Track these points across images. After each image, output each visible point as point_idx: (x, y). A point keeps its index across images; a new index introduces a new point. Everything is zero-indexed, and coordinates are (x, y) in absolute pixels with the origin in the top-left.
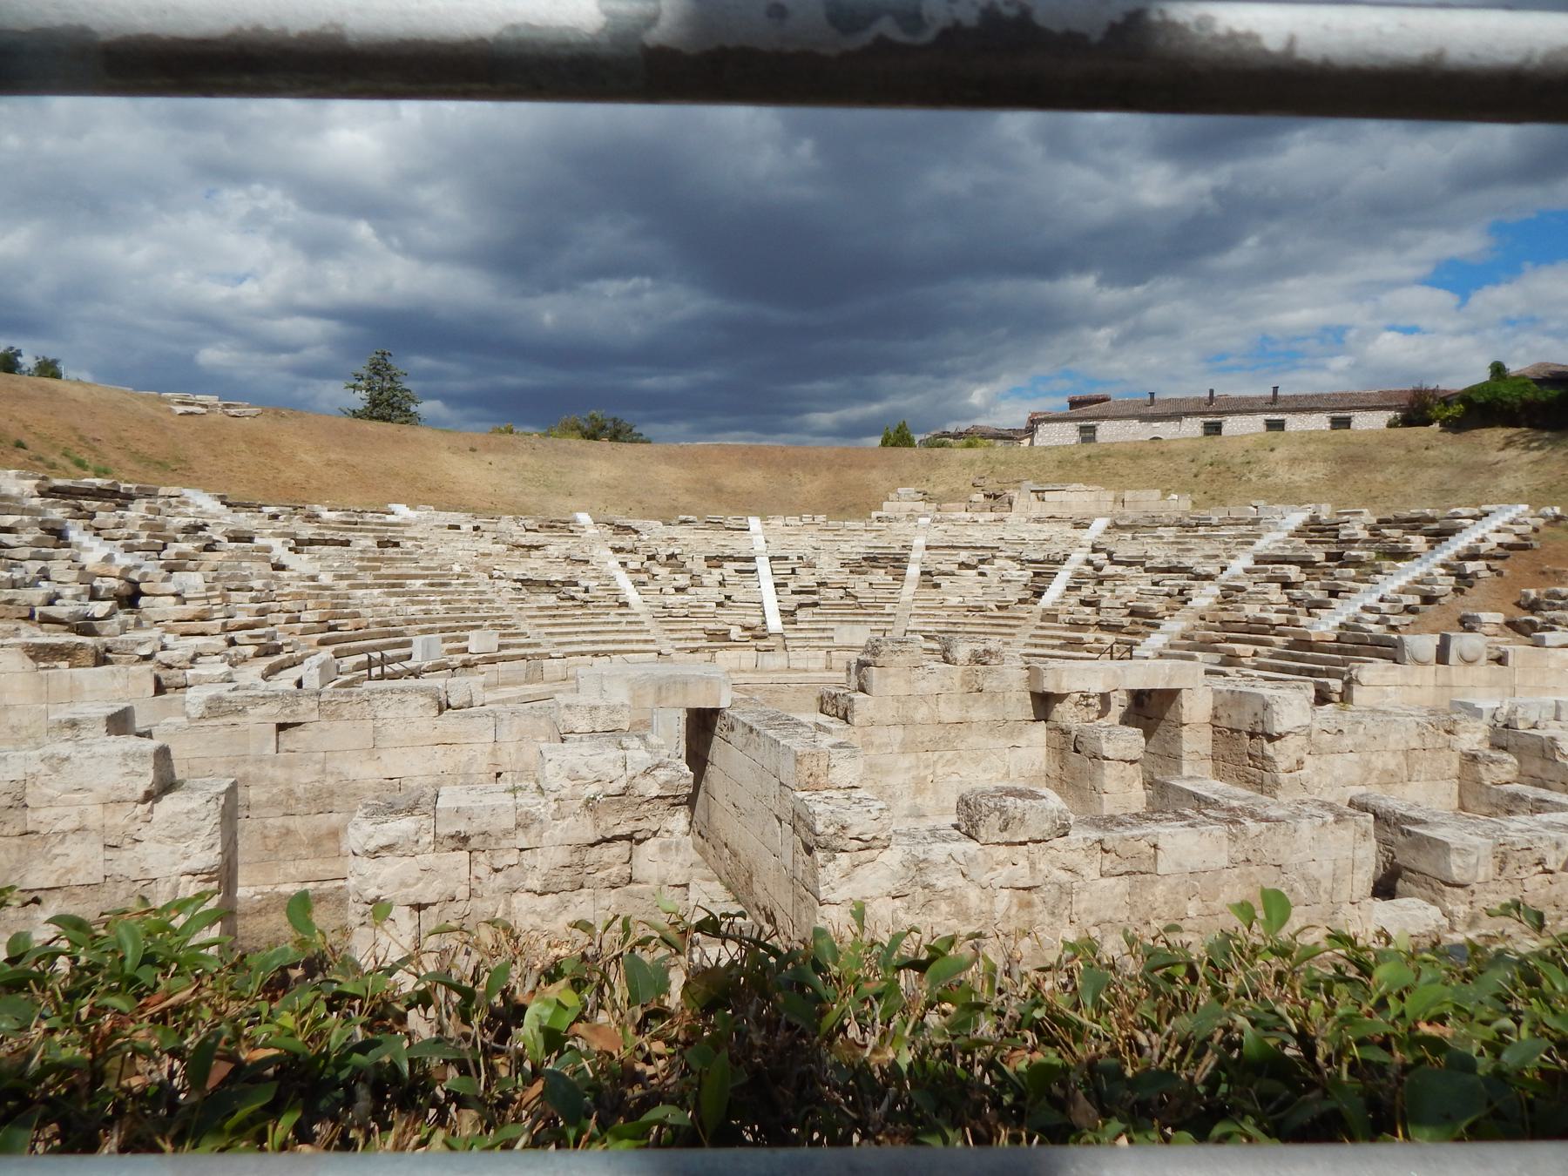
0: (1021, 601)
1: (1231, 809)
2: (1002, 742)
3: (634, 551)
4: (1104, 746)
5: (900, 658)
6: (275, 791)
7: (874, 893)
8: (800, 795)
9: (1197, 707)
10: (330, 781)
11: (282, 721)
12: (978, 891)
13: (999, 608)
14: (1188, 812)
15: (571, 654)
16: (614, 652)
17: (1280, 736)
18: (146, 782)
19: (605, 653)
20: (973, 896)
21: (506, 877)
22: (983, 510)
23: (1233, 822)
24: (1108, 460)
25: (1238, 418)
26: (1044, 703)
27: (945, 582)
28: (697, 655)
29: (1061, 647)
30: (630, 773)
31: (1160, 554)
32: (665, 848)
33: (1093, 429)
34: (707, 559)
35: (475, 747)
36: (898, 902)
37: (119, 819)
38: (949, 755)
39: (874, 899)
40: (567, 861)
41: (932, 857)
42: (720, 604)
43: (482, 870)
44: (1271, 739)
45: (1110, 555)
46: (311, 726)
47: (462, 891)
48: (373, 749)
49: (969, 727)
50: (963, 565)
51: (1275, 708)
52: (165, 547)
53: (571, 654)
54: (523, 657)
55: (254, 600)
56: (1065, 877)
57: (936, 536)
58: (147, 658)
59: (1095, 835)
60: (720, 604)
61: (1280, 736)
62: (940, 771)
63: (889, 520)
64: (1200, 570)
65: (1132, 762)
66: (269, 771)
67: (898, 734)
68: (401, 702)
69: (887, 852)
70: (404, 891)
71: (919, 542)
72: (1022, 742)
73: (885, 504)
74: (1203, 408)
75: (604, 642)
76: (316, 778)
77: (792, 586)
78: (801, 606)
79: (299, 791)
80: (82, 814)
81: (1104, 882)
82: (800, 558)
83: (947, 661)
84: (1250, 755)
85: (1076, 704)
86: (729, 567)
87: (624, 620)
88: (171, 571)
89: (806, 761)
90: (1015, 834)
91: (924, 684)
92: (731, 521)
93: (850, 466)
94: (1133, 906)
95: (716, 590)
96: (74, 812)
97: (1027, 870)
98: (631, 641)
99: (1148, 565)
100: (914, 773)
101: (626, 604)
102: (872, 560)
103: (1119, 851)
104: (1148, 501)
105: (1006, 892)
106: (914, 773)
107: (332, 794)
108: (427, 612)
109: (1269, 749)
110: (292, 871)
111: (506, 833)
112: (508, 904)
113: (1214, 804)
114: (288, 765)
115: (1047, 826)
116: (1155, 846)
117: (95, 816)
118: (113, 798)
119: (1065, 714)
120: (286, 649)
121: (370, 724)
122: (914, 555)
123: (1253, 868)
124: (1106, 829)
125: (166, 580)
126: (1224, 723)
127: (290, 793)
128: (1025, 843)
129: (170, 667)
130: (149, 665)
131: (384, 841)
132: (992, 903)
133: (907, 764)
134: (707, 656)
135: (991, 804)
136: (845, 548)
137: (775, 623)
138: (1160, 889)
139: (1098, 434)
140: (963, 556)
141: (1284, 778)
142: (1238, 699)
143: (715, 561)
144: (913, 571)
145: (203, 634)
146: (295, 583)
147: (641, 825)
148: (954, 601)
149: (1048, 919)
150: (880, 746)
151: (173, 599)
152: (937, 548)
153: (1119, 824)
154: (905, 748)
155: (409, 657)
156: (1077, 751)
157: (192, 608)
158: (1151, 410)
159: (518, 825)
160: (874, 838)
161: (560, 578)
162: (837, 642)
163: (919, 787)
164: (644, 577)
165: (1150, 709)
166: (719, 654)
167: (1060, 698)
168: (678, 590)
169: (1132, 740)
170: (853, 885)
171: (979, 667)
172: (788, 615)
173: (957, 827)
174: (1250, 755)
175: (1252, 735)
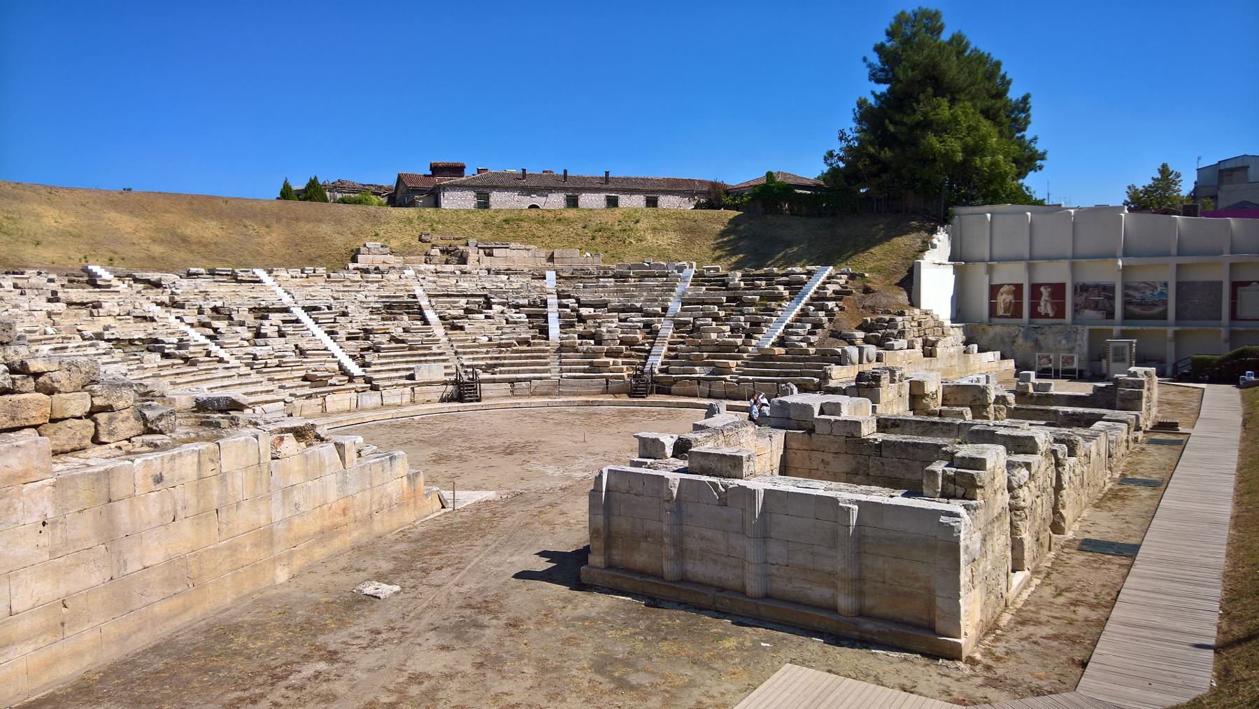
24: (522, 224)
28: (313, 401)
45: (578, 301)
93: (297, 219)
134: (320, 400)
158: (521, 183)
161: (142, 336)
164: (211, 332)
166: (329, 398)
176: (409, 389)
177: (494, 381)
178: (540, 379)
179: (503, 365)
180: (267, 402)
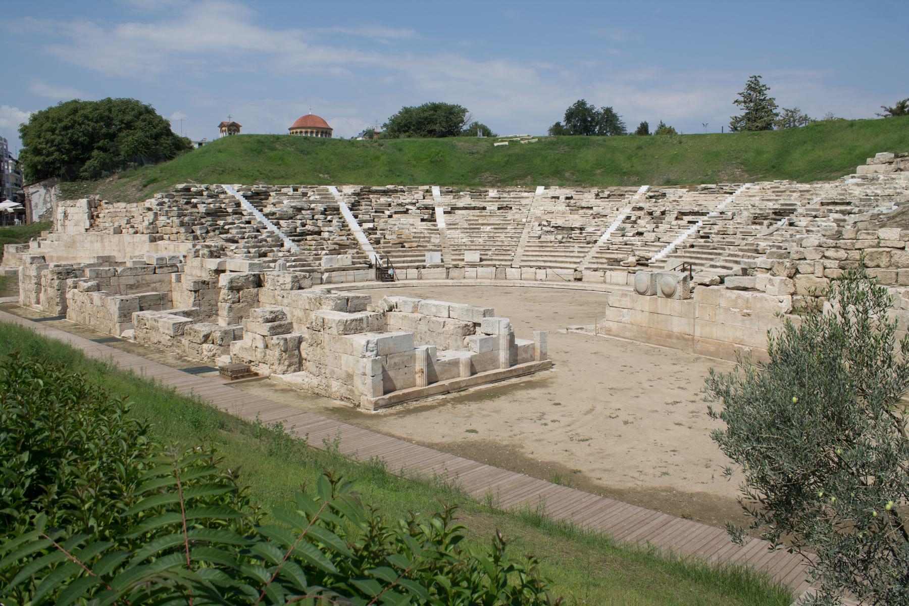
15: (524, 266)
16: (550, 267)
19: (545, 268)
53: (524, 266)
54: (494, 266)
75: (556, 262)
98: (567, 262)
108: (472, 242)
134: (601, 273)
155: (424, 261)
166: (608, 273)
168: (640, 234)
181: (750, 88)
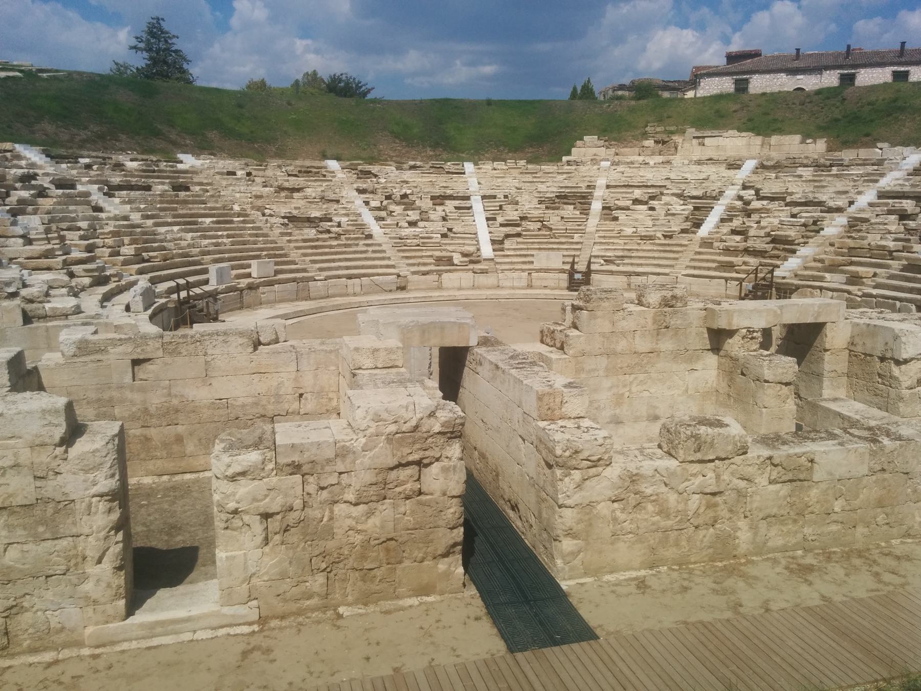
0: (683, 231)
1: (870, 429)
2: (683, 366)
3: (373, 192)
4: (766, 372)
5: (606, 304)
6: (134, 409)
7: (599, 499)
8: (542, 424)
9: (837, 336)
10: (175, 402)
11: (135, 357)
12: (676, 496)
13: (665, 236)
14: (837, 431)
16: (364, 275)
17: (906, 362)
18: (59, 432)
19: (358, 276)
20: (672, 498)
21: (330, 493)
22: (653, 154)
23: (875, 441)
25: (869, 70)
26: (718, 338)
27: (621, 215)
28: (427, 277)
29: (715, 269)
30: (419, 416)
31: (798, 190)
32: (445, 470)
33: (747, 81)
34: (433, 198)
35: (282, 375)
36: (616, 505)
37: (44, 458)
38: (642, 377)
39: (598, 503)
40: (374, 480)
41: (643, 471)
42: (444, 236)
43: (311, 488)
44: (898, 363)
45: (757, 191)
46: (158, 361)
47: (298, 504)
48: (206, 377)
49: (658, 355)
50: (636, 201)
51: (904, 339)
52: (8, 195)
54: (294, 280)
55: (82, 238)
56: (742, 484)
57: (615, 176)
58: (14, 295)
59: (766, 453)
60: (444, 236)
61: (906, 362)
62: (634, 389)
63: (577, 163)
64: (831, 204)
65: (787, 384)
66: (129, 395)
67: (603, 362)
68: (225, 342)
69: (609, 468)
70: (256, 504)
71: (601, 182)
72: (698, 366)
73: (573, 150)
74: (841, 61)
76: (164, 399)
77: (500, 219)
78: (508, 236)
79: (152, 409)
80: (15, 455)
81: (772, 487)
82: (506, 197)
83: (640, 303)
84: (879, 375)
85: (743, 338)
86: (450, 205)
87: (370, 249)
88: (15, 215)
89: (546, 399)
90: (706, 454)
91: (624, 324)
92: (449, 166)
94: (792, 505)
95: (441, 223)
96: (10, 453)
97: (714, 481)
99: (788, 200)
100: (615, 390)
101: (370, 236)
102: (563, 198)
103: (785, 465)
104: (789, 144)
105: (697, 496)
106: (615, 390)
107: (177, 411)
108: (217, 245)
109: (896, 371)
110: (151, 467)
111: (329, 461)
112: (332, 512)
113: (854, 424)
114: (142, 390)
115: (730, 448)
116: (812, 461)
117: (25, 456)
118: (37, 442)
119: (733, 345)
120: (113, 279)
121: (202, 359)
122: (598, 193)
123: (886, 476)
124: (774, 447)
125: (14, 223)
126: (859, 349)
127: (146, 411)
128: (712, 461)
129: (31, 301)
130: (17, 301)
131: (239, 469)
132: (686, 504)
133: (609, 384)
134: (434, 277)
135: (689, 433)
136: (542, 187)
137: (487, 250)
138: (814, 492)
139: (750, 86)
140: (637, 193)
141: (906, 393)
142: (872, 331)
143: (440, 200)
144: (596, 206)
145: (49, 269)
146: (112, 223)
147: (427, 453)
148: (629, 231)
149: (728, 515)
150: (589, 371)
151: (20, 241)
152: (616, 187)
153: (784, 443)
154: (610, 371)
155: (207, 282)
156: (743, 374)
157: (38, 248)
158: (796, 64)
159: (337, 456)
160: (600, 460)
162: (536, 265)
163: (618, 400)
165: (801, 340)
166: (445, 276)
167: (731, 333)
169: (787, 365)
170: (583, 493)
171: (667, 309)
172: (497, 243)
173: (660, 447)
174: (879, 375)
175: (883, 359)
176: (526, 274)
177: (612, 273)
178: (658, 274)
179: (631, 257)
180: (378, 275)
181: (151, 33)
